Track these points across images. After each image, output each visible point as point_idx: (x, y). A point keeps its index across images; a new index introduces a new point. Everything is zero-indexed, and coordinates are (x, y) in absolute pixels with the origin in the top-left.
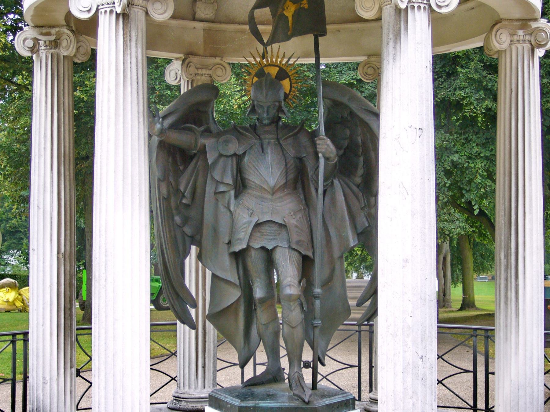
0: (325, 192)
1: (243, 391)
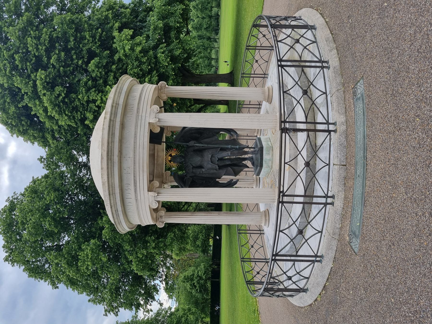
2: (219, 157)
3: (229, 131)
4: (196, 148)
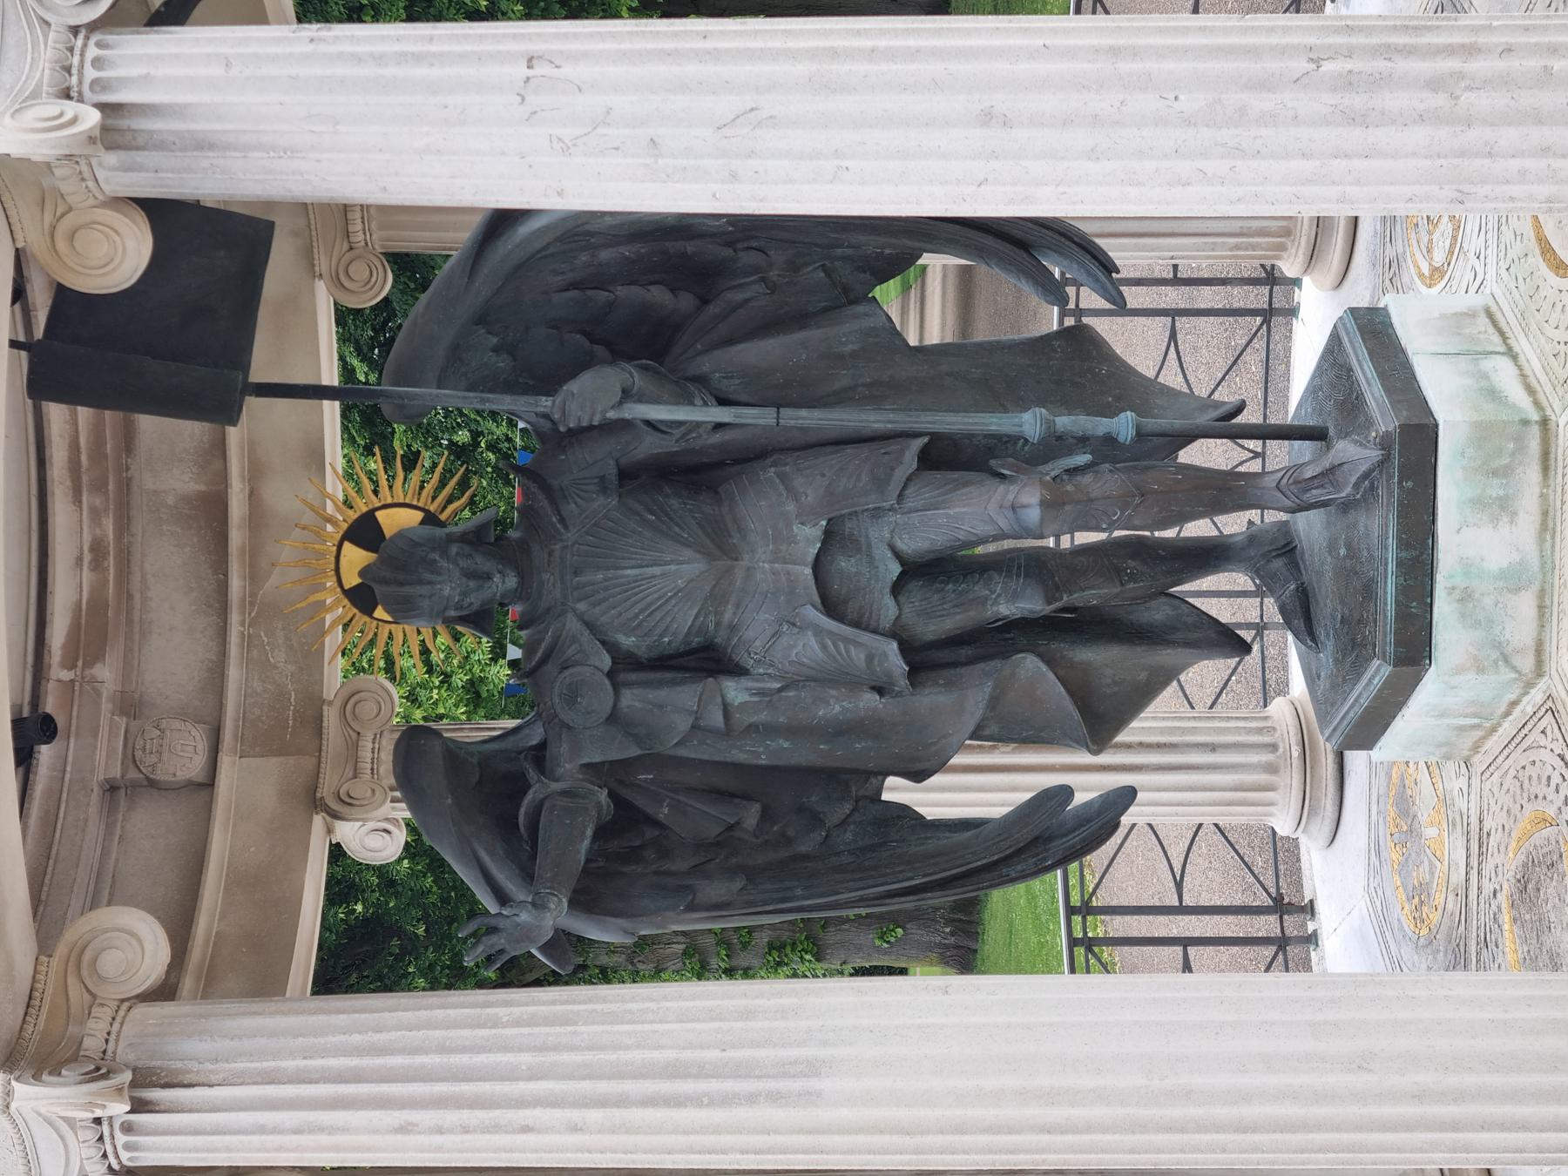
0: (723, 402)
1: (1330, 645)
2: (913, 544)
3: (1016, 244)
4: (648, 447)
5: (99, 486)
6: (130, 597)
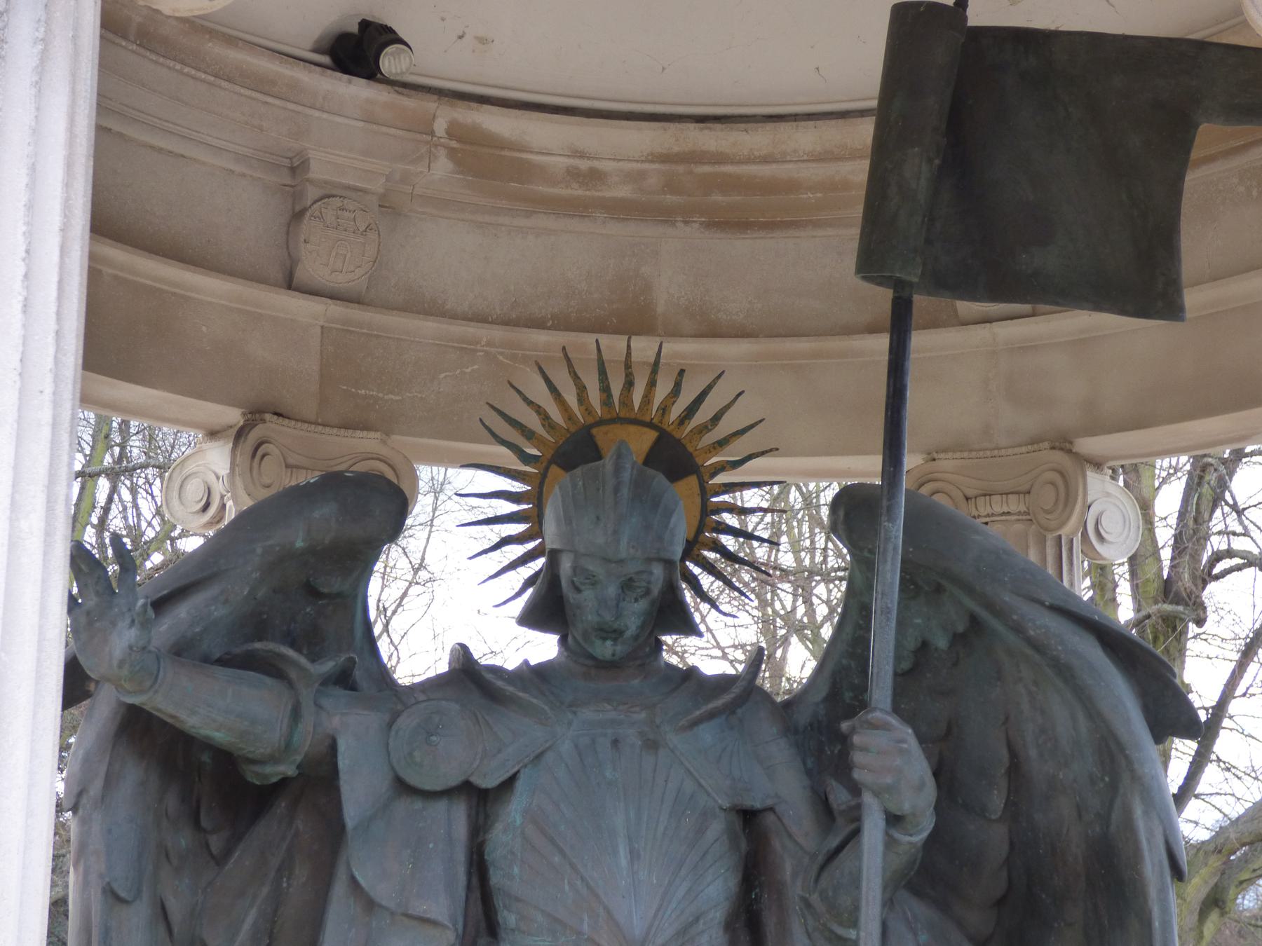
5: (671, 185)
6: (529, 214)
